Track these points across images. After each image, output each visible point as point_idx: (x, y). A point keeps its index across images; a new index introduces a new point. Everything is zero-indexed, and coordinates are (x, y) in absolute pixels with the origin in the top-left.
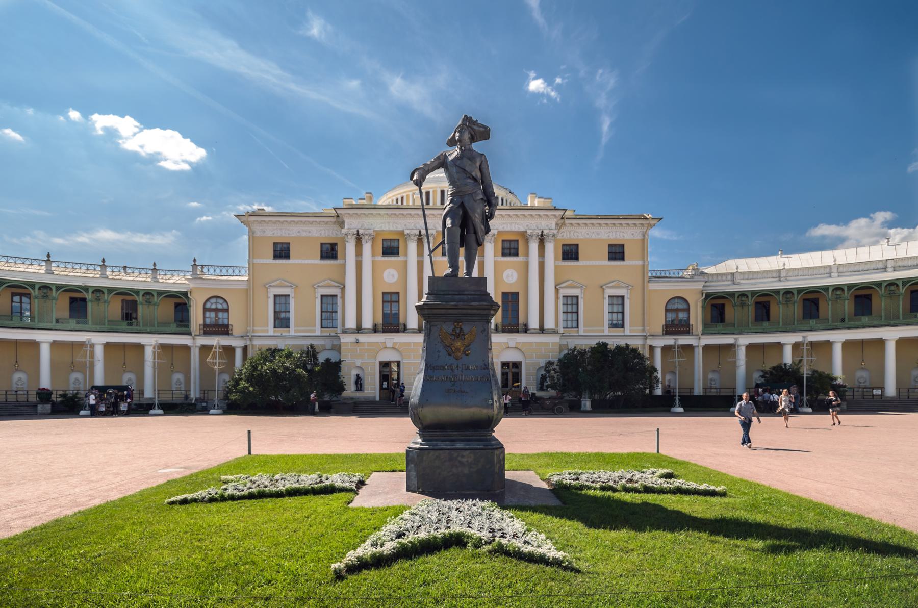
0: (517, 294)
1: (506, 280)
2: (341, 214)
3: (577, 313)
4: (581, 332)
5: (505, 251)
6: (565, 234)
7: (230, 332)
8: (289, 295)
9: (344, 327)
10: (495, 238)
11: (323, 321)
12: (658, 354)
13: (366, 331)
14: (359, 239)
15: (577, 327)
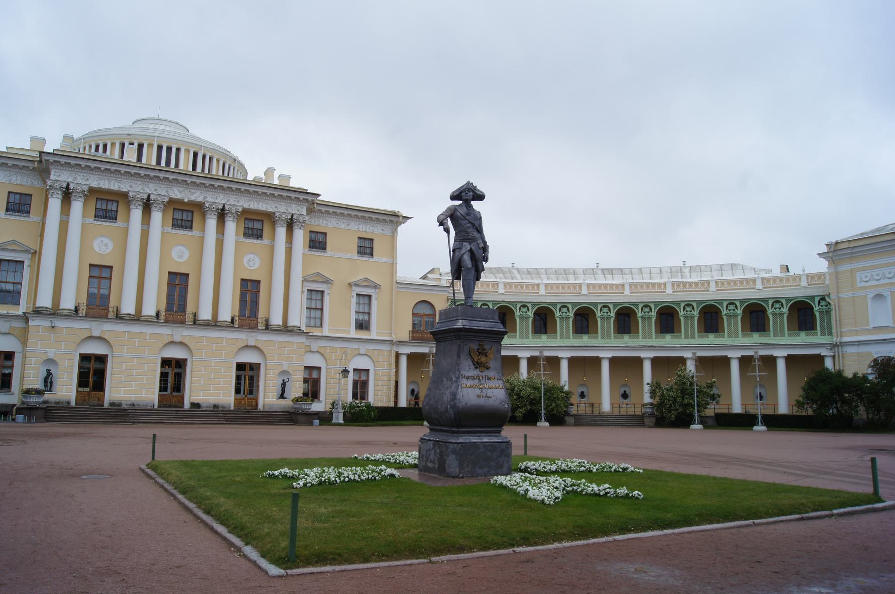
0: (258, 282)
1: (246, 265)
3: (321, 310)
4: (326, 332)
6: (313, 220)
12: (404, 361)
13: (65, 313)
14: (67, 195)
15: (321, 326)
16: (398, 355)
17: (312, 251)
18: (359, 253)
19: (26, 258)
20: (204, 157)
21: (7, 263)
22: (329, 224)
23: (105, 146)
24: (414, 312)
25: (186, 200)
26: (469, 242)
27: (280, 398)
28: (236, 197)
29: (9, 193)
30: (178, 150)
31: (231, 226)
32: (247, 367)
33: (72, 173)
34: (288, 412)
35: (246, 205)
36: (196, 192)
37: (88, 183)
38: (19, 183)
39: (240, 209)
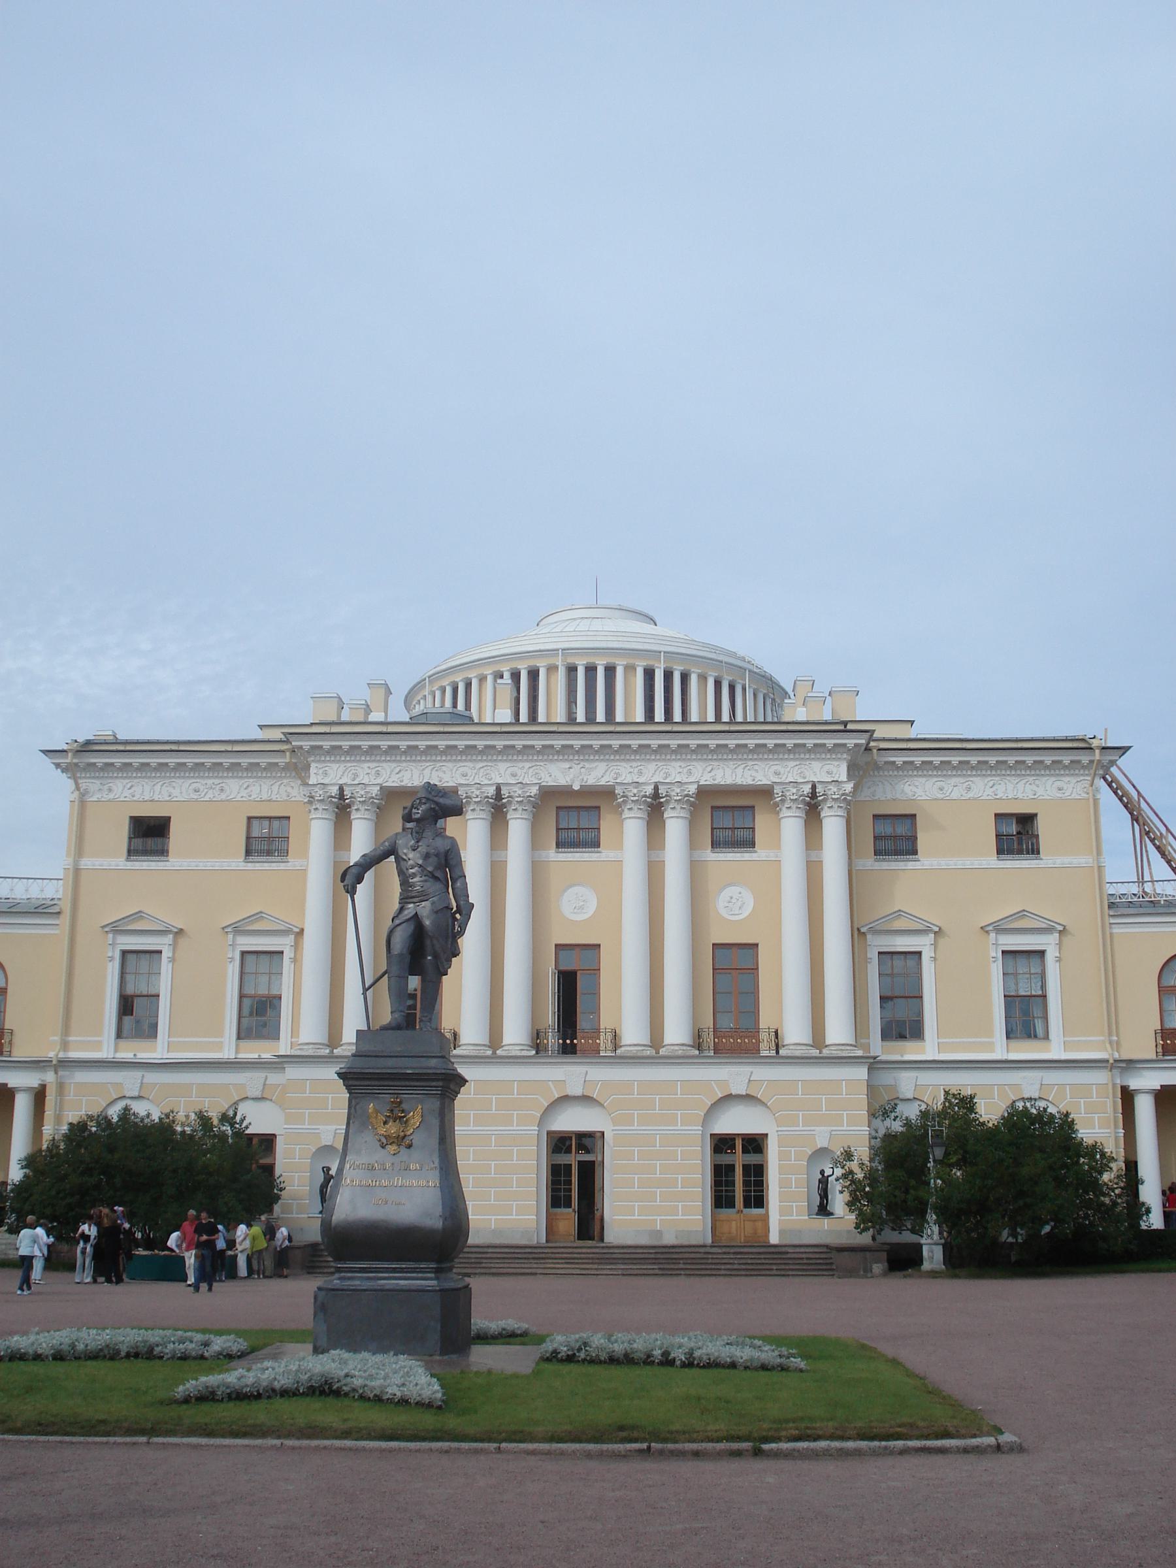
1: (723, 913)
2: (301, 747)
5: (720, 834)
7: (6, 1048)
8: (160, 952)
9: (298, 1037)
10: (692, 804)
11: (243, 1020)
12: (1145, 1109)
16: (1128, 1097)
17: (884, 860)
18: (1000, 851)
19: (284, 944)
20: (668, 675)
21: (254, 957)
22: (919, 792)
23: (468, 685)
24: (1165, 983)
25: (576, 787)
26: (414, 903)
27: (817, 1214)
28: (683, 764)
29: (249, 818)
30: (610, 671)
31: (675, 827)
32: (739, 1144)
33: (349, 765)
34: (827, 1246)
35: (707, 779)
36: (597, 766)
37: (379, 781)
38: (265, 797)
39: (692, 789)
